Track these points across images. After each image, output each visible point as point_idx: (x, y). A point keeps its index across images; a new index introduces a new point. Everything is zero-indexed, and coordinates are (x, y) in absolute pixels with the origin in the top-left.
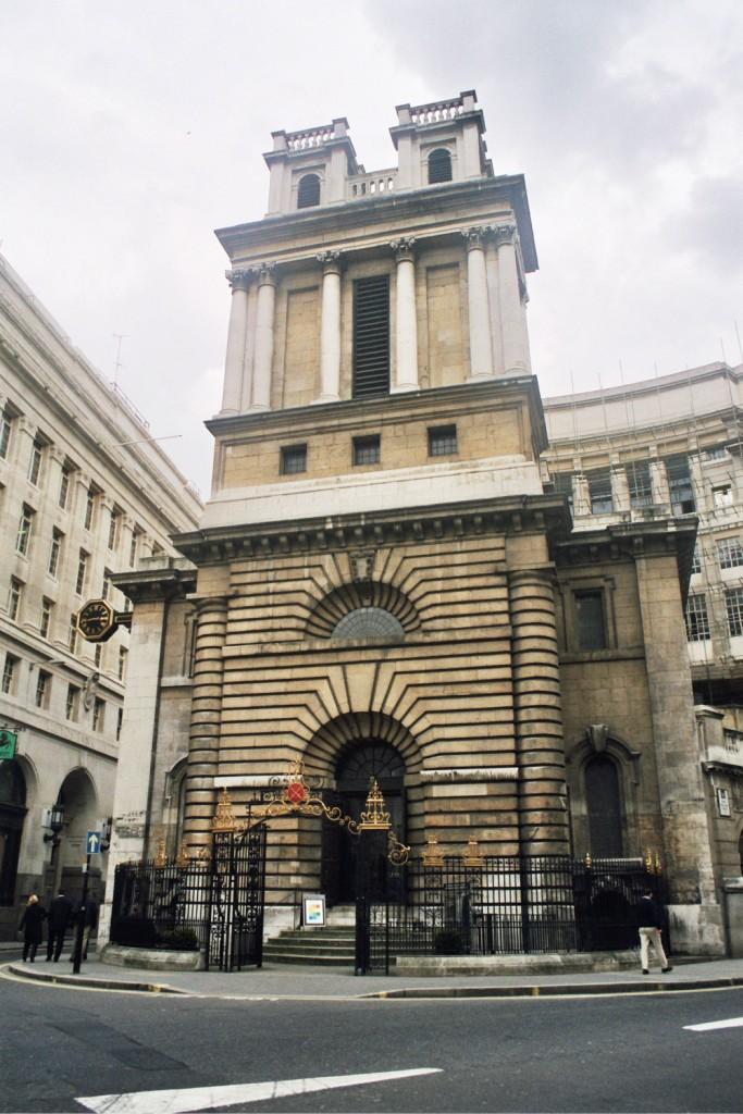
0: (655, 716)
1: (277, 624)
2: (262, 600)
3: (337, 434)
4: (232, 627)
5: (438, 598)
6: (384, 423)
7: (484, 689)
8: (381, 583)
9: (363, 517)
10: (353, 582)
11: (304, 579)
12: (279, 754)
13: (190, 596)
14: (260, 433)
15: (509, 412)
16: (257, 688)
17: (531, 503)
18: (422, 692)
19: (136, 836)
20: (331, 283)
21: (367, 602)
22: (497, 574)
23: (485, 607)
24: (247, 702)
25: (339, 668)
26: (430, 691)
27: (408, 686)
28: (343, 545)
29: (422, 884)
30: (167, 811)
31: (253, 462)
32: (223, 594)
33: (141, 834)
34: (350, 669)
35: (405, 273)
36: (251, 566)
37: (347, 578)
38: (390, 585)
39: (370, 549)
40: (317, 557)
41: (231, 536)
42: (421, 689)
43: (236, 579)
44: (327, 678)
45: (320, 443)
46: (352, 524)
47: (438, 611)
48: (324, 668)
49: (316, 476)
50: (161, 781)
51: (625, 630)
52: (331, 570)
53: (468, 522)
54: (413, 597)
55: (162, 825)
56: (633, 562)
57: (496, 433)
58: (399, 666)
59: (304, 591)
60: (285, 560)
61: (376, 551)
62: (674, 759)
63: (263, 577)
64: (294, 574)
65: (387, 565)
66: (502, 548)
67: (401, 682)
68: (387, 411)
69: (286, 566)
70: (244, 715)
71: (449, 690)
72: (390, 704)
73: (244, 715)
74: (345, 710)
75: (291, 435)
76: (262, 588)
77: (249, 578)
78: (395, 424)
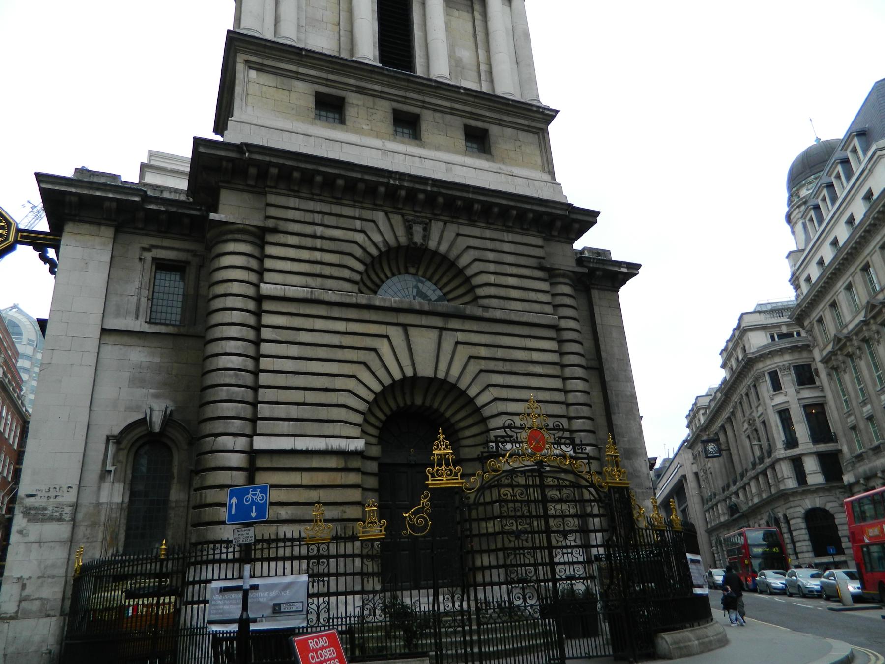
0: (614, 417)
1: (327, 271)
2: (308, 242)
3: (377, 100)
5: (492, 279)
6: (424, 105)
7: (538, 369)
8: (435, 253)
9: (430, 182)
10: (409, 245)
11: (355, 230)
12: (336, 413)
13: (213, 216)
14: (293, 68)
15: (531, 135)
16: (305, 337)
17: (574, 213)
18: (484, 365)
19: (60, 520)
21: (412, 270)
22: (541, 268)
23: (532, 296)
24: (294, 350)
26: (492, 365)
27: (470, 357)
28: (400, 206)
29: (486, 563)
30: (106, 486)
31: (282, 95)
32: (259, 223)
33: (67, 517)
34: (412, 331)
36: (292, 202)
38: (444, 258)
39: (426, 218)
40: (369, 212)
41: (281, 161)
42: (483, 362)
43: (272, 212)
44: (387, 337)
45: (360, 103)
46: (418, 186)
47: (492, 291)
48: (383, 327)
50: (98, 446)
52: (384, 229)
53: (522, 215)
54: (469, 272)
55: (98, 505)
57: (523, 148)
58: (461, 337)
59: (356, 243)
60: (333, 206)
61: (430, 221)
63: (309, 217)
64: (343, 222)
65: (442, 237)
66: (541, 247)
67: (463, 353)
68: (430, 96)
69: (334, 212)
70: (288, 365)
71: (508, 367)
72: (455, 372)
73: (288, 365)
74: (409, 373)
75: (327, 82)
76: (309, 229)
77: (290, 214)
78: (435, 110)
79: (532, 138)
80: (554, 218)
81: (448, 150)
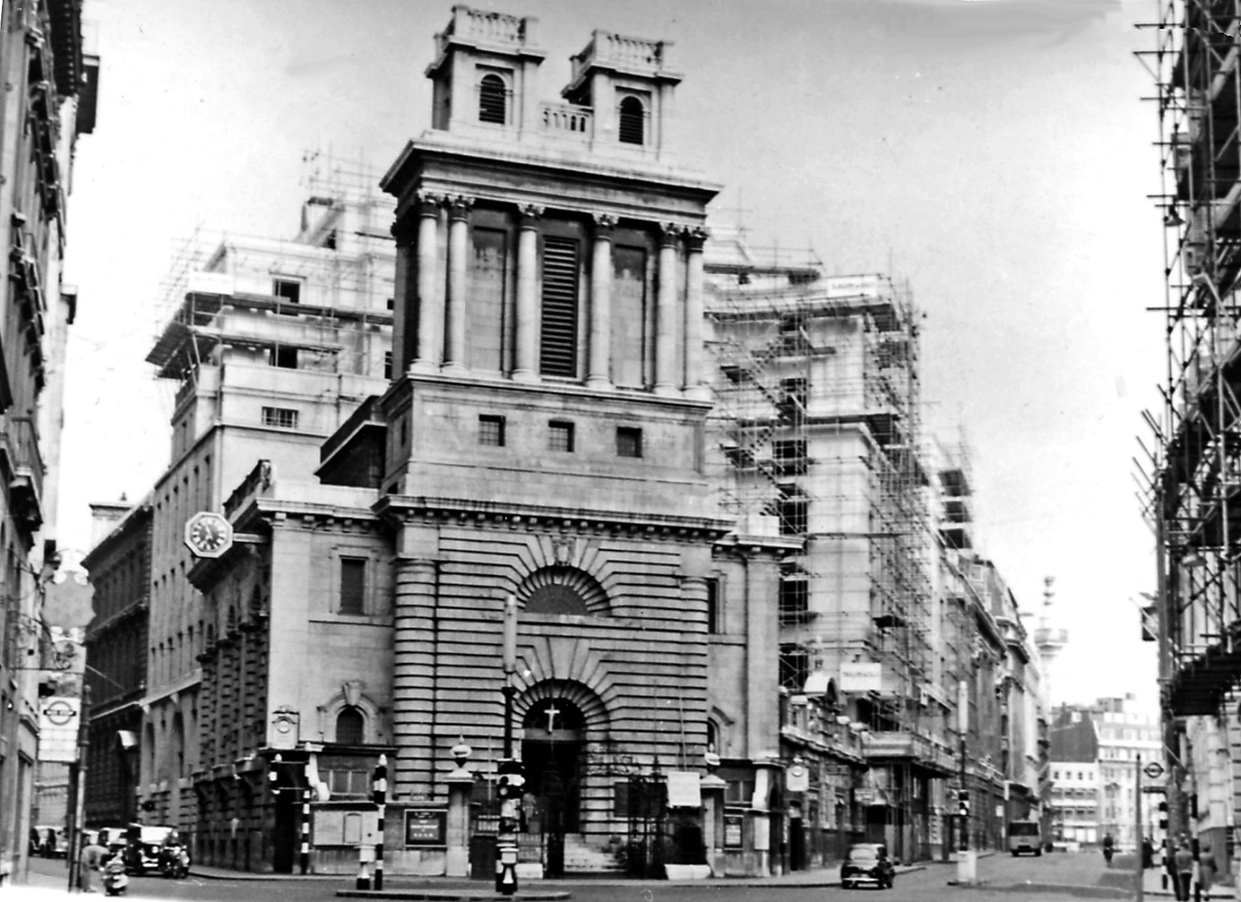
4: (443, 590)
20: (529, 242)
25: (543, 640)
35: (603, 254)
37: (551, 562)
43: (445, 544)
44: (532, 647)
46: (565, 516)
58: (594, 644)
65: (586, 554)
75: (491, 404)
79: (688, 430)
80: (690, 530)
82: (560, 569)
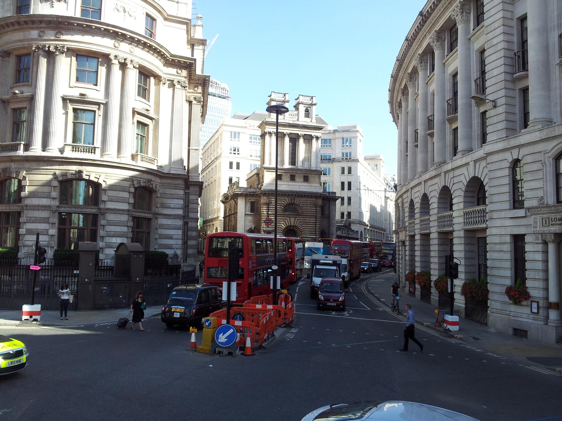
49: (284, 181)
51: (327, 212)
56: (329, 201)
62: (332, 234)
65: (297, 201)
67: (299, 221)
79: (318, 176)
81: (300, 182)
82: (293, 204)
